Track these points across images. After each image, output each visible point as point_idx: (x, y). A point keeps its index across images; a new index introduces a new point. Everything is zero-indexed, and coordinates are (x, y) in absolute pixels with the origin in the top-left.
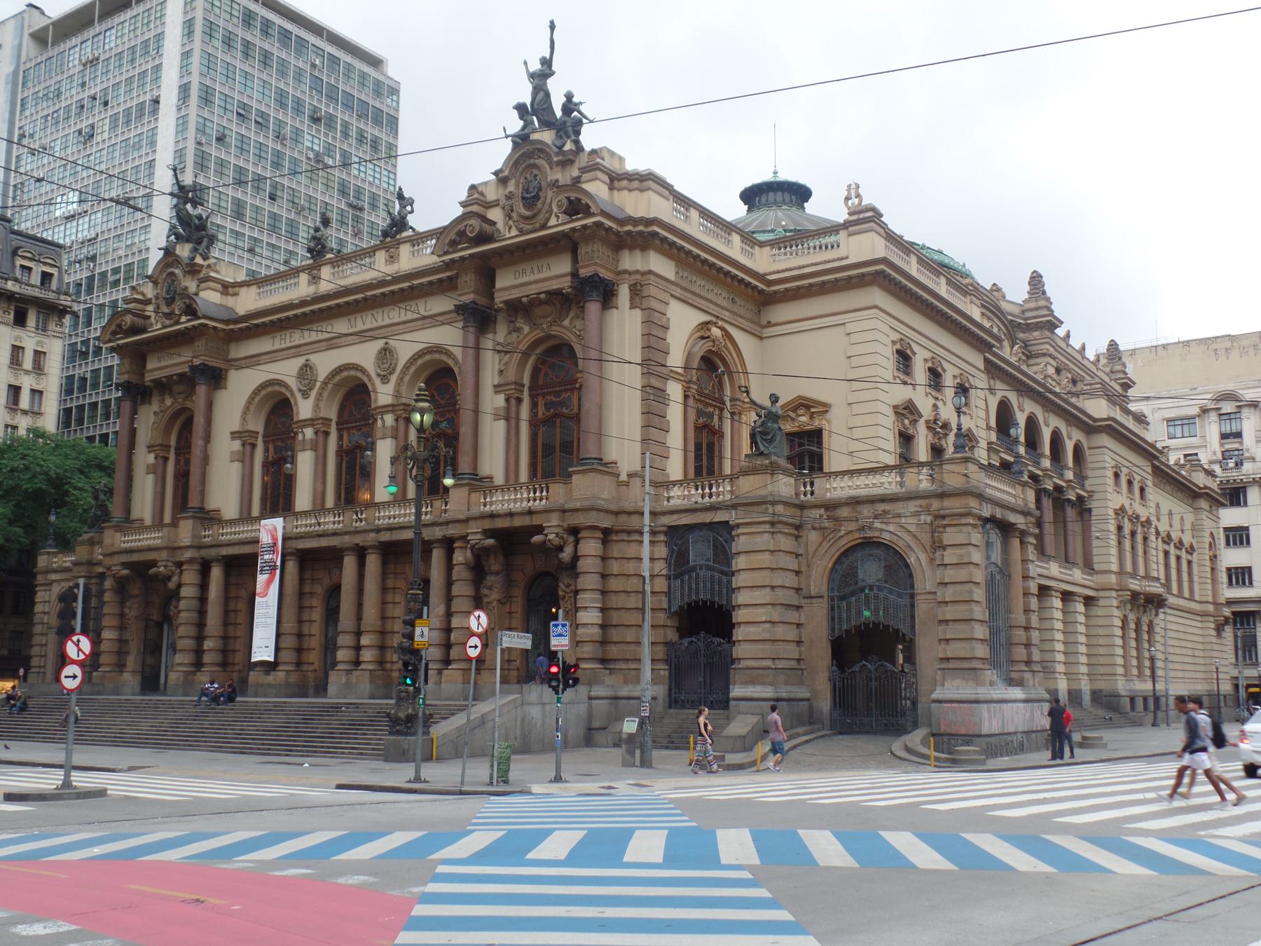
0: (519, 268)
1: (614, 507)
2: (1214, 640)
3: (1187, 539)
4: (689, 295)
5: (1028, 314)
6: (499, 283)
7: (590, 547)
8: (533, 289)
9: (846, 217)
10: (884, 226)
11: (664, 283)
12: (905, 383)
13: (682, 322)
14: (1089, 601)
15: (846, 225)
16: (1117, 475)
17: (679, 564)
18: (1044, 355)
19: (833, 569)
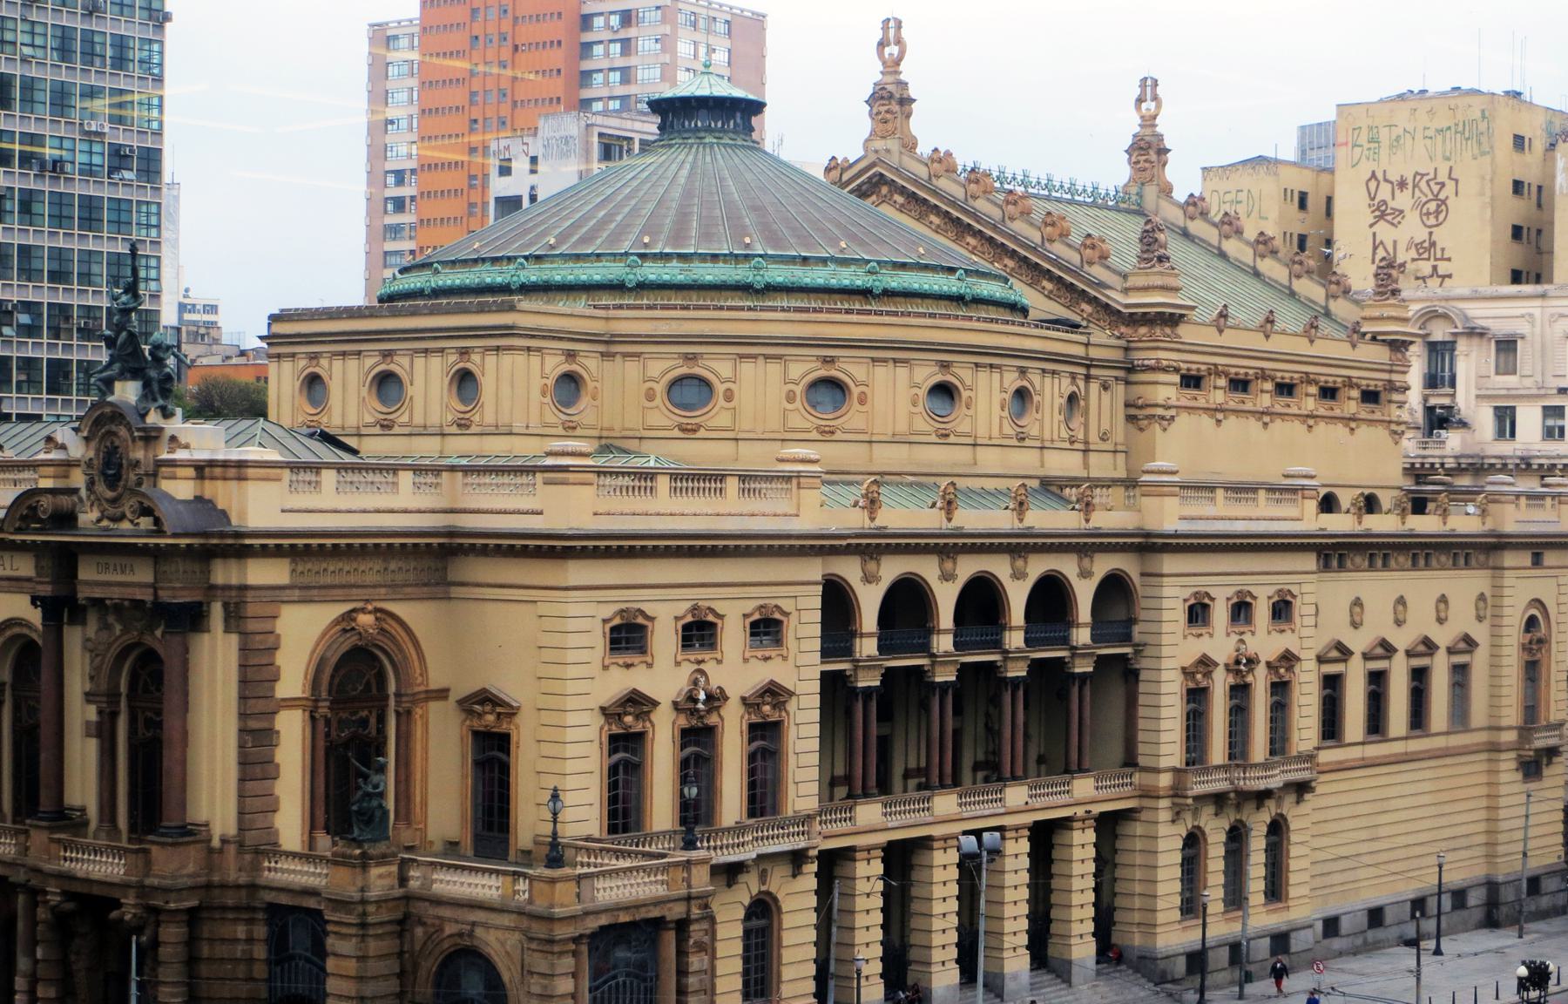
1: (202, 880)
7: (172, 933)
8: (116, 593)
11: (269, 593)
13: (302, 634)
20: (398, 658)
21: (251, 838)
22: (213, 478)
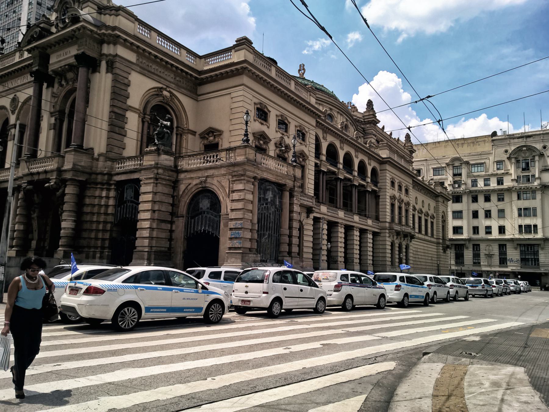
0: (59, 53)
2: (442, 254)
3: (430, 213)
4: (146, 72)
5: (365, 117)
6: (52, 61)
9: (236, 43)
10: (253, 49)
12: (262, 124)
14: (375, 234)
15: (234, 47)
16: (393, 183)
17: (120, 201)
18: (371, 134)
19: (190, 204)
20: (178, 113)
21: (112, 155)
22: (105, 15)
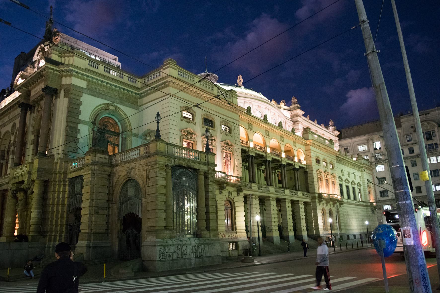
14: (305, 204)
22: (64, 57)
